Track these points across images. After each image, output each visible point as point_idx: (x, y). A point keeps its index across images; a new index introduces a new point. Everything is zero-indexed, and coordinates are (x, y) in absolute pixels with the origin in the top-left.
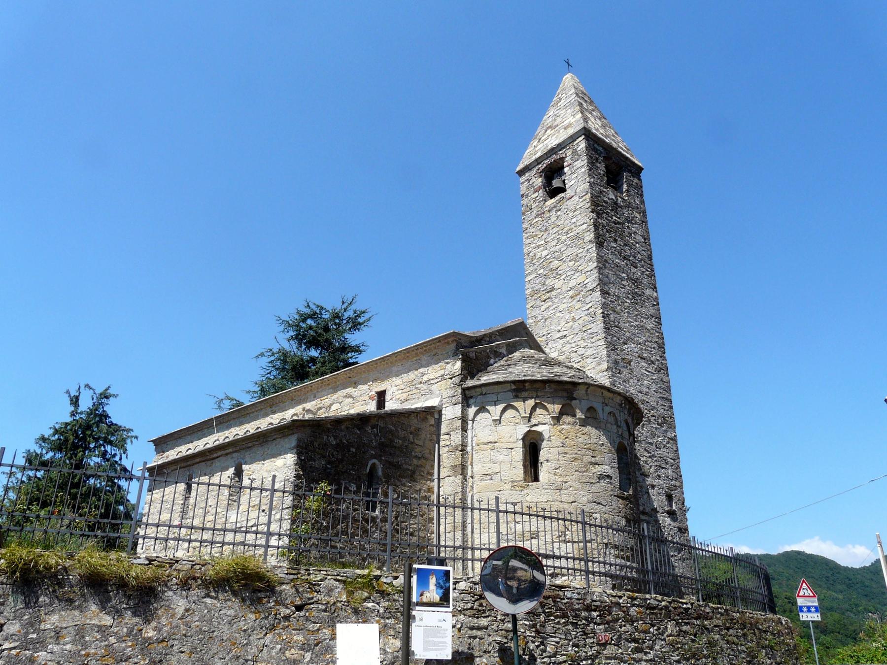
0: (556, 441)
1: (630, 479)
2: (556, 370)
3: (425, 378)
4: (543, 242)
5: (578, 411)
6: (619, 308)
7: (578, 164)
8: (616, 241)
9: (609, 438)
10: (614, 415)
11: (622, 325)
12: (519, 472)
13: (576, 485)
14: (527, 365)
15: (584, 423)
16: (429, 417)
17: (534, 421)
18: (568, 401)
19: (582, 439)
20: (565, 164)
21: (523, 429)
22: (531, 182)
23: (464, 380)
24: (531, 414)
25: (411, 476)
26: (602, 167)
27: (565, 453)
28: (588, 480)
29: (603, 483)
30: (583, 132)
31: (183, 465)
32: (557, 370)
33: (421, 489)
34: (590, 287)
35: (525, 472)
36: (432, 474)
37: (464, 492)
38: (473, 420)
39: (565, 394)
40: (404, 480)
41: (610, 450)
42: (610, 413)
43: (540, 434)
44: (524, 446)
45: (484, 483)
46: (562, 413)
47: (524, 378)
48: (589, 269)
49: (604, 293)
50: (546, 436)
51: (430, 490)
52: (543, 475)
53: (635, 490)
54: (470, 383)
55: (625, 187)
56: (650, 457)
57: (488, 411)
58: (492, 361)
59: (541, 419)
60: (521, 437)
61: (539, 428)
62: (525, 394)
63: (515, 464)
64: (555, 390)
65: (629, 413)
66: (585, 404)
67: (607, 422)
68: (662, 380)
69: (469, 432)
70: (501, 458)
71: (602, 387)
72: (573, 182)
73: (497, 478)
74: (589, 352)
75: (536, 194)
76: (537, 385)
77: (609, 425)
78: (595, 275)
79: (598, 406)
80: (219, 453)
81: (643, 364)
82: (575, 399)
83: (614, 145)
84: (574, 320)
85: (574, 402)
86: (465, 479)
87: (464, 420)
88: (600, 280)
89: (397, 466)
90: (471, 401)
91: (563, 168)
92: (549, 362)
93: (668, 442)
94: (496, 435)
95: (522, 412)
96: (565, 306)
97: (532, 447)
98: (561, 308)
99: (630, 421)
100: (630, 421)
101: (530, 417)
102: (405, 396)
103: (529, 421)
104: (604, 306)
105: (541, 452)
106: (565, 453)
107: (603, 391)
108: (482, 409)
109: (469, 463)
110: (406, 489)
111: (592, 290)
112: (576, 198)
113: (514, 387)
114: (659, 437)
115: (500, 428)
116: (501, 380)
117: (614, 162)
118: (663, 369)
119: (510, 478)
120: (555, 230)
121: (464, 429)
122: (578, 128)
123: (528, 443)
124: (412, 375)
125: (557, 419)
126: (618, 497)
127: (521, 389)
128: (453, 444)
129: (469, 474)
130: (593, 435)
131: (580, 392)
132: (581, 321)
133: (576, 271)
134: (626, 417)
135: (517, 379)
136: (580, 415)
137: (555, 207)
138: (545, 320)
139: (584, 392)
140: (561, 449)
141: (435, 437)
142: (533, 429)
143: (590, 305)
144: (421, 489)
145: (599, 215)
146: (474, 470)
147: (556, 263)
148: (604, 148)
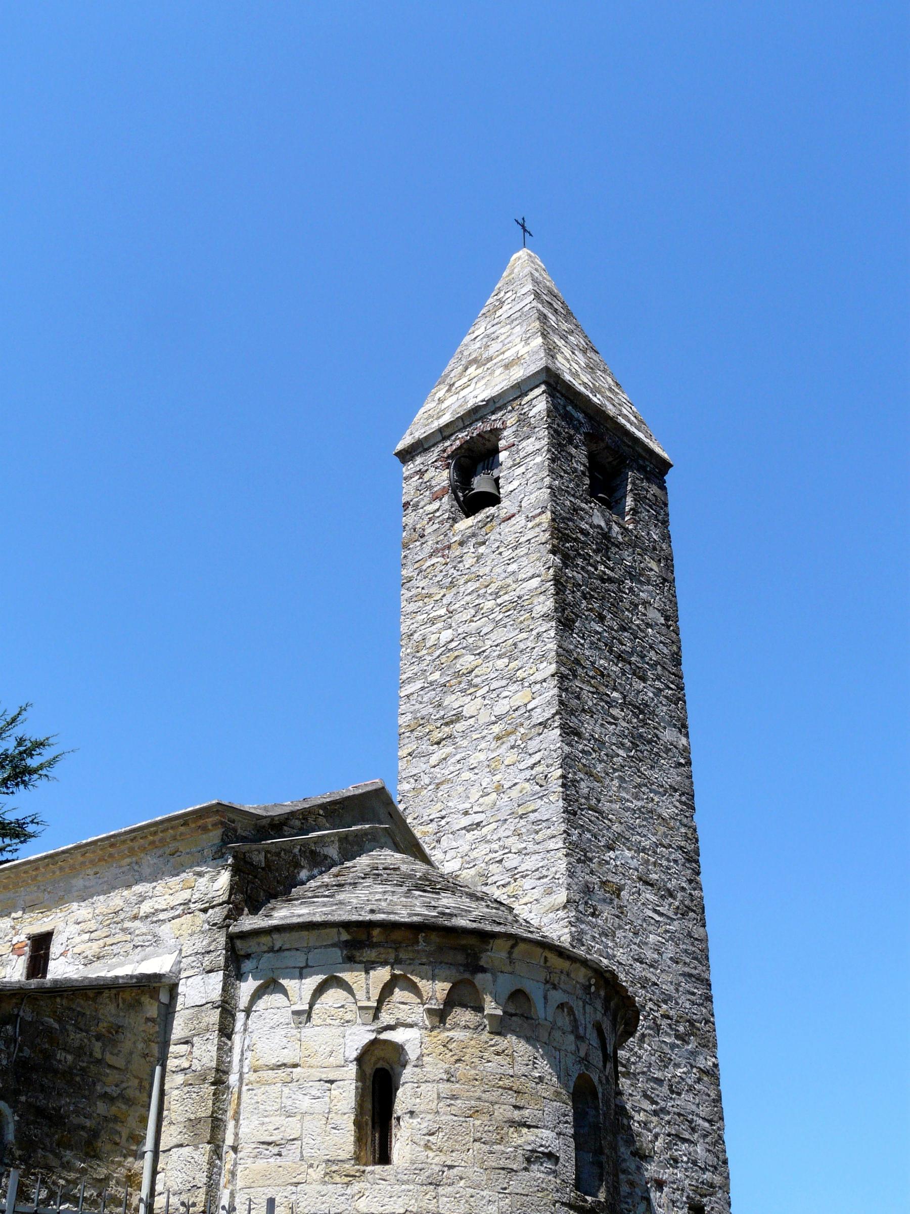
0: (435, 1067)
1: (600, 1165)
2: (444, 902)
3: (146, 908)
4: (443, 611)
5: (488, 998)
6: (600, 767)
7: (530, 445)
8: (601, 618)
9: (556, 1064)
10: (571, 1011)
11: (605, 806)
12: (344, 1140)
13: (475, 1173)
14: (380, 888)
15: (500, 1028)
16: (145, 999)
17: (386, 1018)
18: (467, 976)
19: (494, 1065)
20: (502, 444)
21: (360, 1036)
22: (427, 477)
23: (233, 915)
24: (380, 1001)
25: (89, 1143)
26: (580, 457)
27: (454, 1097)
28: (502, 1163)
29: (538, 1172)
30: (543, 377)
32: (447, 901)
33: (108, 1178)
34: (539, 716)
35: (359, 1140)
36: (140, 1140)
37: (212, 1187)
38: (248, 1011)
39: (460, 958)
40: (68, 1155)
41: (557, 1093)
42: (561, 1006)
43: (398, 1049)
44: (361, 1076)
45: (261, 1164)
46: (450, 1002)
47: (369, 917)
48: (539, 677)
49: (570, 733)
50: (412, 1053)
51: (132, 1180)
52: (400, 1149)
53: (614, 1191)
54: (248, 922)
55: (629, 502)
56: (655, 1113)
57: (284, 992)
58: (304, 874)
59: (403, 1012)
60: (354, 1054)
61: (397, 1036)
62: (370, 954)
63: (336, 1119)
64: (440, 949)
65: (606, 1009)
66: (507, 984)
67: (554, 1026)
68: (689, 935)
69: (237, 1038)
70: (305, 1103)
71: (545, 945)
72: (515, 484)
73: (292, 1153)
74: (530, 863)
75: (436, 505)
76: (397, 935)
77: (557, 1034)
78: (551, 691)
79: (535, 990)
81: (649, 895)
82: (483, 970)
83: (611, 410)
84: (499, 789)
85: (480, 976)
86: (217, 1152)
87: (226, 1009)
88: (561, 702)
89: (56, 1119)
90: (247, 965)
91: (496, 451)
92: (432, 883)
93: (699, 1080)
94: (298, 1048)
95: (360, 994)
96: (482, 756)
97: (379, 1078)
98: (473, 761)
99: (606, 1025)
100: (606, 1025)
101: (378, 1009)
102: (95, 947)
103: (376, 1017)
104: (567, 761)
105: (400, 1093)
106: (454, 1097)
107: (550, 955)
108: (270, 986)
109: (230, 1113)
110: (72, 1176)
111: (544, 724)
112: (520, 520)
113: (345, 937)
114: (677, 1066)
115: (308, 1031)
116: (317, 918)
117: (607, 447)
118: (694, 910)
119: (322, 1155)
120: (471, 586)
121: (226, 1031)
122: (534, 368)
123: (369, 1071)
124: (117, 899)
125: (440, 1016)
126: (570, 1206)
127: (361, 941)
128: (196, 1065)
129: (229, 1140)
130: (520, 1056)
131: (496, 954)
132: (514, 793)
133: (512, 679)
134: (599, 1016)
135: (355, 918)
136: (491, 1007)
137: (474, 535)
138: (438, 785)
139: (504, 955)
140: (445, 1087)
141: (155, 1049)
142: (385, 1036)
143: (537, 757)
144: (108, 1178)
145: (567, 560)
146: (243, 1130)
147: (468, 661)
148: (586, 415)
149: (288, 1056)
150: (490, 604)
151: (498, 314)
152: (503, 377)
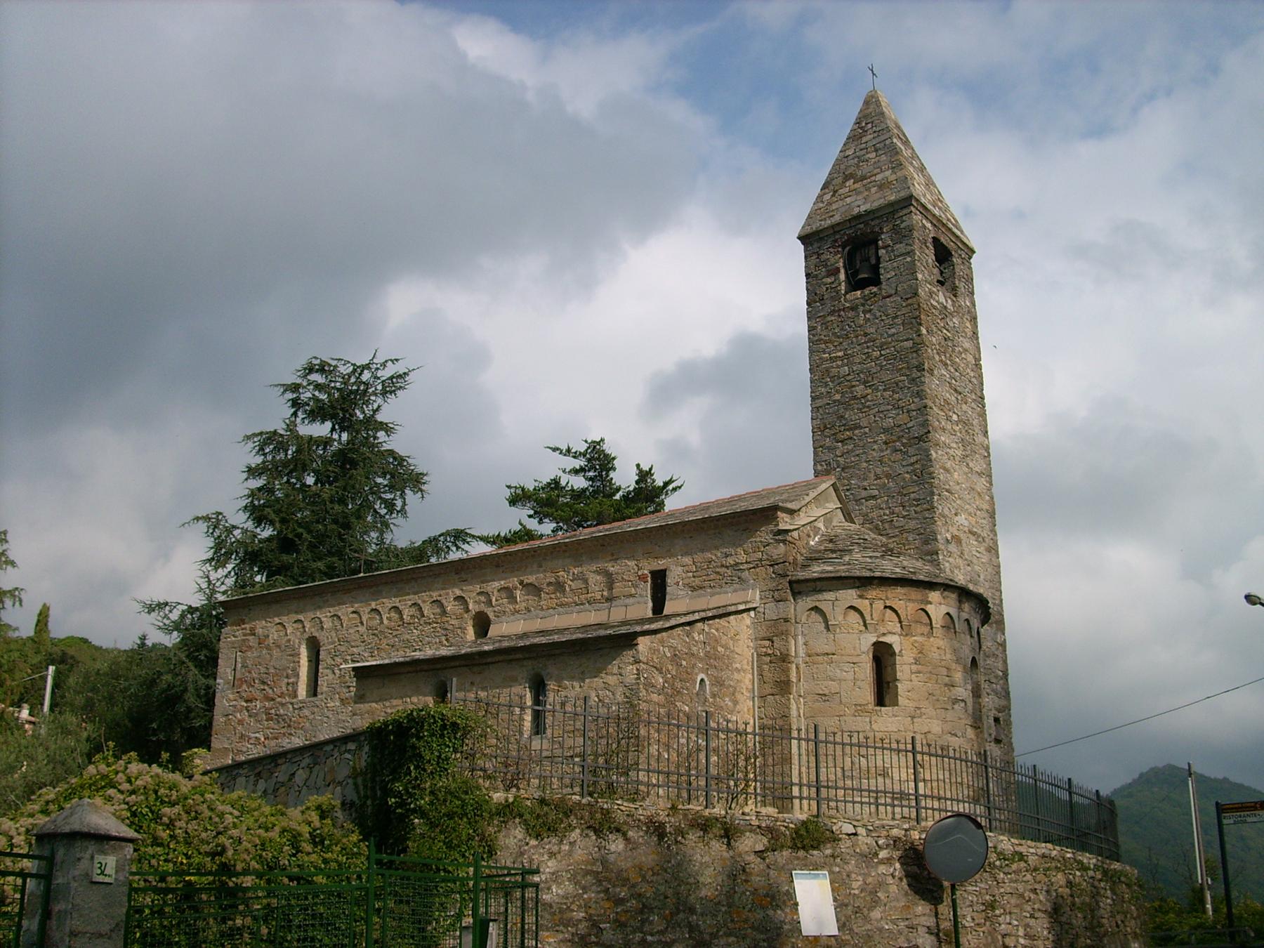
3: (731, 561)
31: (425, 667)
50: (897, 649)
80: (501, 658)
118: (993, 550)
124: (715, 555)
140: (914, 667)
147: (860, 390)
149: (827, 649)
150: (877, 354)
151: (864, 140)
152: (878, 195)
